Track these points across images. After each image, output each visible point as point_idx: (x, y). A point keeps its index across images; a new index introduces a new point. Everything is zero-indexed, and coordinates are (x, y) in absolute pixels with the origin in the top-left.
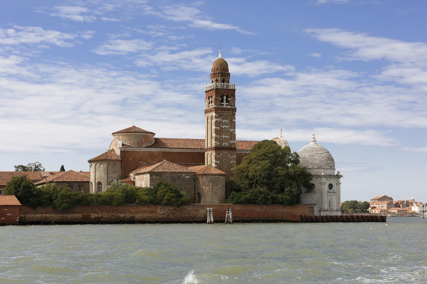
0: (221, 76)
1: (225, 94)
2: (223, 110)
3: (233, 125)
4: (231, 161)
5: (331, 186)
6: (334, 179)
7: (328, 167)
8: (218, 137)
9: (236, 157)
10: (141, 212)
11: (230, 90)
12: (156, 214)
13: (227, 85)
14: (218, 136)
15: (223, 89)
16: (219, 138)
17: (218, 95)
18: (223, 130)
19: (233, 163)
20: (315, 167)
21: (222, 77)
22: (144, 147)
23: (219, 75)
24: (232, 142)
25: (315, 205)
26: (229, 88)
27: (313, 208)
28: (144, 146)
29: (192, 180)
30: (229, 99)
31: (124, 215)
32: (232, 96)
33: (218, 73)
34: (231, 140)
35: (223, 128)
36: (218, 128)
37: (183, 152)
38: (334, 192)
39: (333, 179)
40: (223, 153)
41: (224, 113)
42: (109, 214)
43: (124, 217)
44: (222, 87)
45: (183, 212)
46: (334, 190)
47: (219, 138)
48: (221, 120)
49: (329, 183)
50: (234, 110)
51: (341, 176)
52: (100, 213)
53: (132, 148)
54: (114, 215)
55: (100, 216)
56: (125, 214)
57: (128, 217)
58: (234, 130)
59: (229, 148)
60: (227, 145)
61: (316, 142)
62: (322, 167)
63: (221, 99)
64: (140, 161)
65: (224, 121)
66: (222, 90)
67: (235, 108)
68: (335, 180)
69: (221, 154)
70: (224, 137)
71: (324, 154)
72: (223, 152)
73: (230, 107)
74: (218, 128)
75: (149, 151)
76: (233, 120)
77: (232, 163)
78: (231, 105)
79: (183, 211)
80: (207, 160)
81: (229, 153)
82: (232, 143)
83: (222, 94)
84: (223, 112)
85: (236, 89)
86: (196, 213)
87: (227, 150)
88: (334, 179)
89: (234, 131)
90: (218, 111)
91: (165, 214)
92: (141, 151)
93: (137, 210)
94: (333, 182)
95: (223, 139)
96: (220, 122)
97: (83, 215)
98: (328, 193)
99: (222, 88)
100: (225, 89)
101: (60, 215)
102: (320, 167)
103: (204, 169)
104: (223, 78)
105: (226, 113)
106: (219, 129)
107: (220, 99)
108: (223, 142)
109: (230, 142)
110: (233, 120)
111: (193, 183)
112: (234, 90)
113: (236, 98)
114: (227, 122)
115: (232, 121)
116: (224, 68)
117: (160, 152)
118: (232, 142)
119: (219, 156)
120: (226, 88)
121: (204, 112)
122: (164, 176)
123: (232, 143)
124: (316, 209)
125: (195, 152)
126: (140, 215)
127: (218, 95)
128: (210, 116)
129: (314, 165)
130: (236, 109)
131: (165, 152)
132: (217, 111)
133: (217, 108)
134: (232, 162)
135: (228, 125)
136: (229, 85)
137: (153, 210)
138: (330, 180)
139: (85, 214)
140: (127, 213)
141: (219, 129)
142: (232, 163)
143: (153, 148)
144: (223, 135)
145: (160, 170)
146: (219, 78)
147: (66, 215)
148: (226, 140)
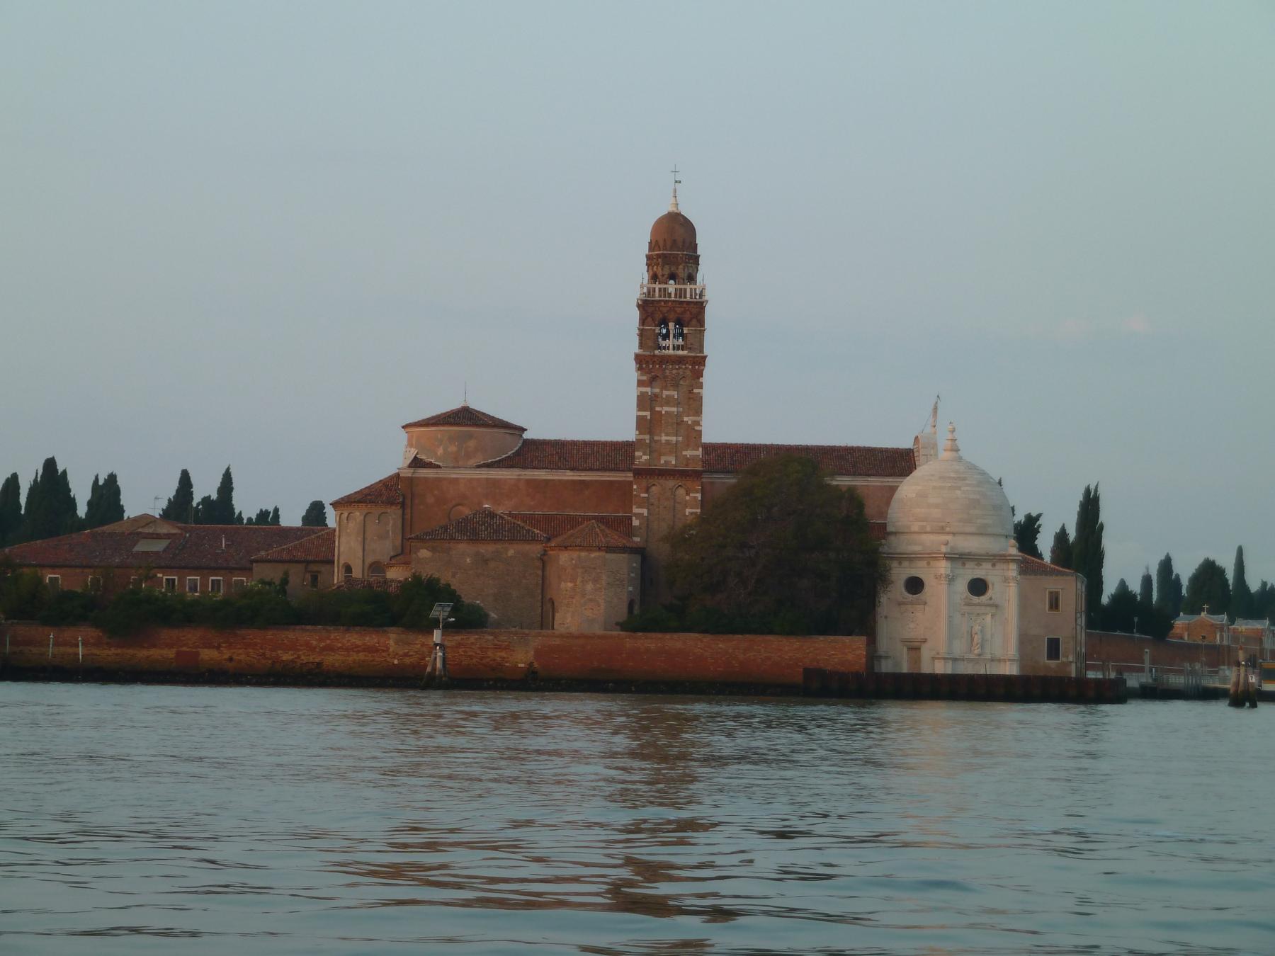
0: (663, 266)
1: (672, 316)
2: (661, 363)
3: (694, 404)
4: (687, 510)
6: (994, 565)
8: (645, 440)
10: (341, 648)
11: (688, 303)
12: (384, 654)
13: (681, 289)
14: (647, 437)
15: (666, 302)
17: (649, 319)
18: (663, 418)
20: (928, 529)
21: (667, 267)
22: (470, 467)
23: (660, 260)
25: (925, 641)
26: (685, 297)
27: (918, 649)
28: (473, 462)
29: (539, 564)
31: (292, 655)
32: (694, 322)
33: (657, 255)
35: (663, 413)
36: (648, 414)
37: (591, 481)
38: (991, 602)
40: (662, 486)
42: (251, 650)
43: (292, 661)
44: (665, 297)
45: (463, 651)
46: (991, 599)
47: (648, 441)
48: (657, 390)
49: (970, 577)
50: (701, 361)
52: (225, 647)
53: (434, 471)
54: (264, 654)
56: (294, 654)
57: (303, 660)
59: (679, 471)
60: (673, 462)
61: (959, 452)
64: (460, 507)
65: (666, 393)
66: (663, 303)
67: (702, 355)
70: (664, 438)
71: (962, 489)
72: (662, 481)
73: (685, 353)
74: (648, 414)
75: (487, 478)
76: (696, 391)
77: (687, 514)
78: (690, 348)
79: (464, 649)
81: (680, 486)
83: (661, 316)
84: (664, 366)
86: (503, 654)
87: (672, 478)
88: (994, 565)
89: (698, 423)
90: (648, 366)
91: (412, 655)
92: (464, 479)
93: (328, 642)
96: (656, 396)
97: (178, 654)
98: (966, 607)
99: (662, 299)
100: (674, 301)
101: (116, 652)
102: (943, 527)
104: (670, 269)
105: (672, 369)
106: (649, 418)
107: (654, 330)
109: (684, 453)
110: (696, 391)
111: (540, 572)
114: (676, 397)
115: (690, 392)
116: (674, 241)
117: (519, 480)
118: (688, 453)
119: (646, 495)
120: (676, 296)
124: (926, 653)
126: (337, 655)
127: (649, 319)
129: (924, 524)
130: (705, 358)
131: (535, 480)
132: (644, 366)
133: (645, 356)
135: (678, 404)
137: (376, 643)
138: (974, 569)
139: (184, 649)
140: (302, 650)
143: (498, 469)
144: (663, 434)
146: (660, 269)
147: (131, 651)
148: (675, 449)
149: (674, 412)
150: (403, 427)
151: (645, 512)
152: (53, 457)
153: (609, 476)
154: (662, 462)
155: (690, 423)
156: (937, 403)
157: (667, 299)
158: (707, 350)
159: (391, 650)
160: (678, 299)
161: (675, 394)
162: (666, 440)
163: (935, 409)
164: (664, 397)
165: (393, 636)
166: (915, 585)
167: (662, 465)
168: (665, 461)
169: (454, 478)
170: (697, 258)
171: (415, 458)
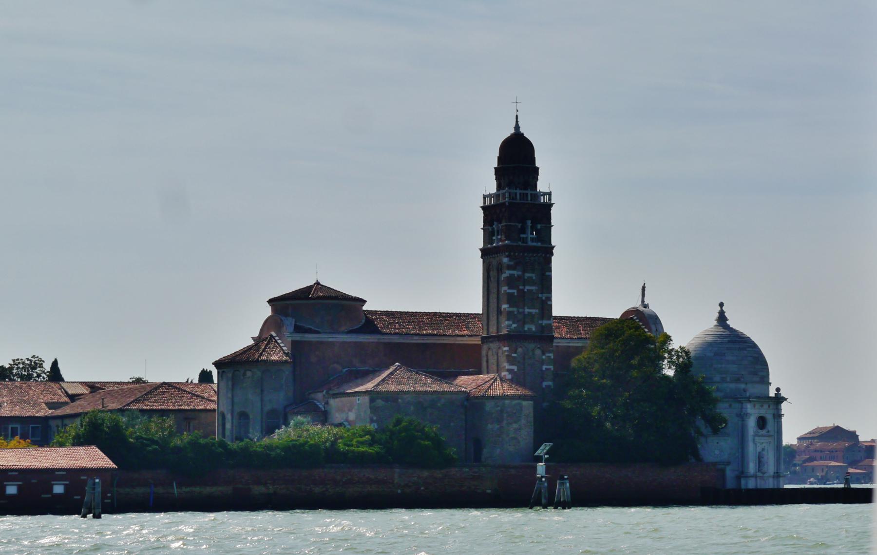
5: (762, 422)
6: (769, 406)
7: (757, 379)
9: (552, 357)
14: (515, 309)
16: (516, 313)
19: (547, 369)
24: (545, 322)
25: (728, 463)
34: (542, 319)
35: (526, 290)
36: (515, 291)
39: (766, 406)
40: (526, 347)
41: (527, 258)
47: (516, 313)
48: (520, 273)
49: (757, 415)
51: (785, 399)
55: (271, 491)
58: (548, 295)
60: (534, 329)
62: (742, 379)
65: (527, 275)
67: (550, 246)
68: (771, 407)
69: (520, 350)
70: (527, 310)
73: (539, 244)
76: (547, 274)
77: (544, 369)
80: (487, 362)
82: (544, 324)
85: (554, 204)
92: (337, 342)
94: (766, 412)
95: (525, 315)
96: (519, 277)
103: (488, 384)
106: (516, 294)
108: (524, 323)
109: (540, 322)
110: (547, 274)
112: (549, 206)
113: (552, 224)
114: (534, 278)
115: (543, 274)
117: (377, 343)
118: (545, 322)
122: (400, 400)
123: (544, 324)
125: (457, 342)
128: (494, 262)
129: (724, 376)
132: (512, 254)
134: (544, 367)
139: (240, 486)
141: (516, 294)
142: (544, 369)
144: (526, 308)
145: (393, 388)
149: (533, 290)
151: (515, 368)
153: (437, 340)
154: (526, 329)
155: (544, 298)
157: (525, 202)
158: (554, 242)
159: (396, 481)
160: (532, 202)
161: (533, 276)
162: (528, 312)
163: (644, 289)
165: (397, 470)
167: (525, 331)
168: (528, 329)
169: (331, 342)
170: (538, 168)
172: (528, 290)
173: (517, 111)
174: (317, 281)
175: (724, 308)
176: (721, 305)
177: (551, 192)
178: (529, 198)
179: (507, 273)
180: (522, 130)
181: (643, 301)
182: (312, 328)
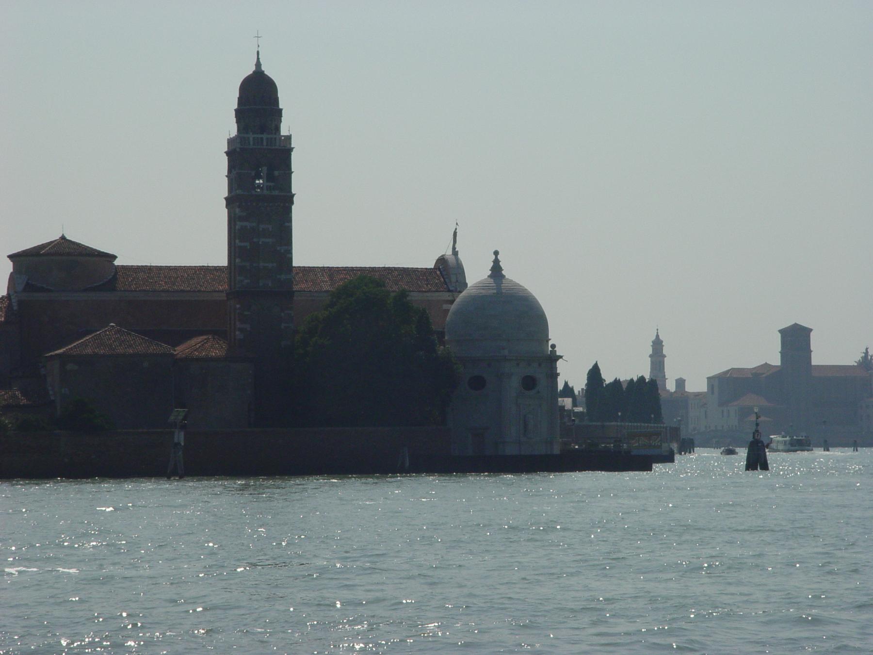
6: (540, 365)
13: (271, 139)
30: (276, 173)
35: (260, 243)
36: (247, 244)
48: (254, 224)
50: (289, 199)
63: (253, 174)
70: (262, 264)
73: (276, 193)
76: (287, 224)
89: (289, 251)
109: (278, 277)
110: (287, 224)
112: (286, 152)
113: (293, 170)
114: (270, 229)
120: (267, 145)
121: (224, 202)
136: (275, 139)
145: (89, 351)
150: (10, 257)
152: (780, 331)
154: (261, 284)
155: (282, 251)
156: (456, 229)
160: (269, 147)
163: (455, 234)
164: (261, 229)
166: (478, 383)
170: (281, 110)
171: (27, 284)
172: (262, 242)
173: (259, 46)
174: (63, 234)
175: (499, 257)
176: (496, 253)
177: (291, 135)
178: (265, 143)
179: (239, 225)
180: (263, 68)
181: (454, 248)
182: (44, 286)
